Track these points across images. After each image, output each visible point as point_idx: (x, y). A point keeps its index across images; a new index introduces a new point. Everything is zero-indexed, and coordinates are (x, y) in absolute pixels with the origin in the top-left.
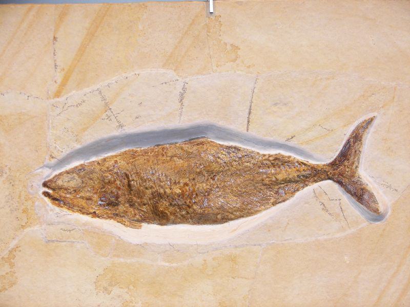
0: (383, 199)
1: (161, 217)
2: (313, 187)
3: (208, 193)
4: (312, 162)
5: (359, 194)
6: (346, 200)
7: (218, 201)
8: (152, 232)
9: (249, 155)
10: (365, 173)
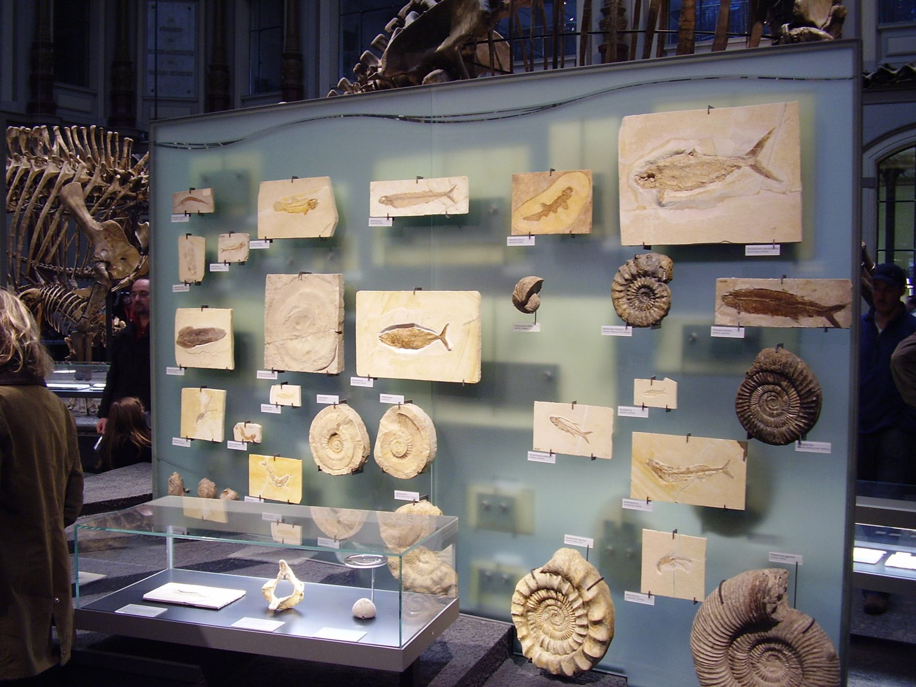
0: (450, 345)
1: (403, 347)
2: (436, 341)
3: (414, 341)
4: (436, 334)
5: (446, 344)
6: (443, 344)
7: (415, 343)
8: (403, 351)
9: (423, 332)
10: (447, 338)
